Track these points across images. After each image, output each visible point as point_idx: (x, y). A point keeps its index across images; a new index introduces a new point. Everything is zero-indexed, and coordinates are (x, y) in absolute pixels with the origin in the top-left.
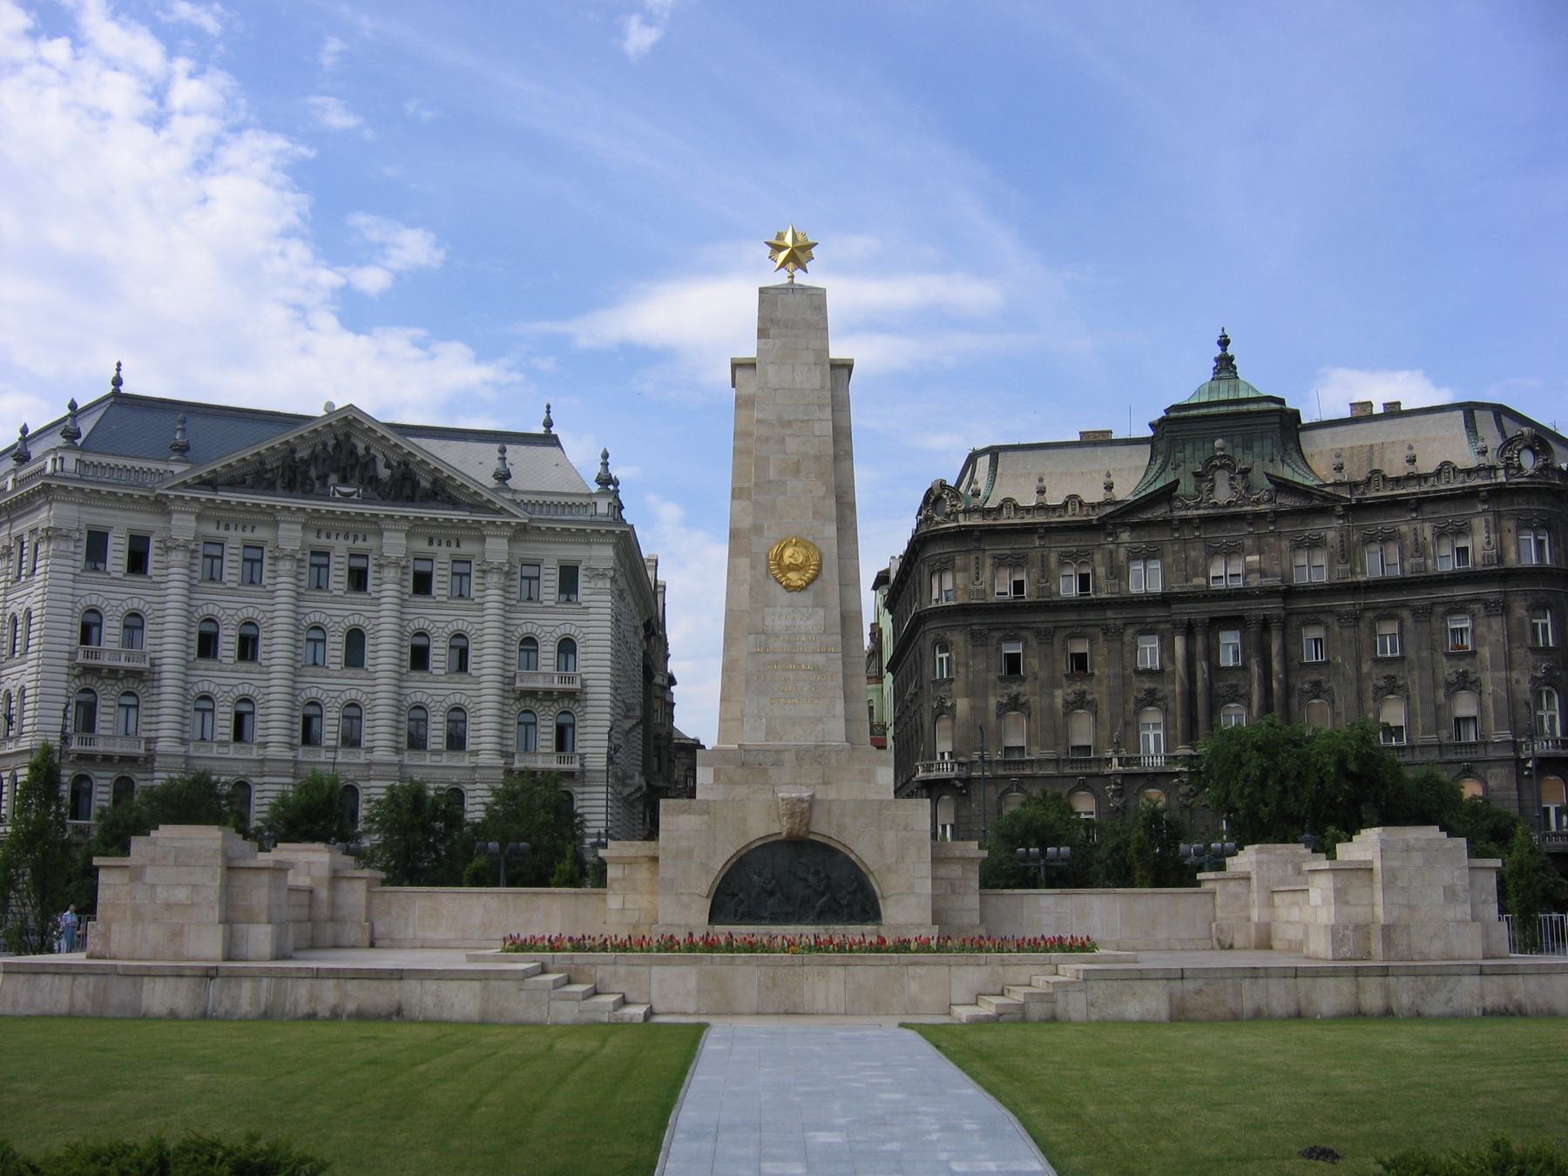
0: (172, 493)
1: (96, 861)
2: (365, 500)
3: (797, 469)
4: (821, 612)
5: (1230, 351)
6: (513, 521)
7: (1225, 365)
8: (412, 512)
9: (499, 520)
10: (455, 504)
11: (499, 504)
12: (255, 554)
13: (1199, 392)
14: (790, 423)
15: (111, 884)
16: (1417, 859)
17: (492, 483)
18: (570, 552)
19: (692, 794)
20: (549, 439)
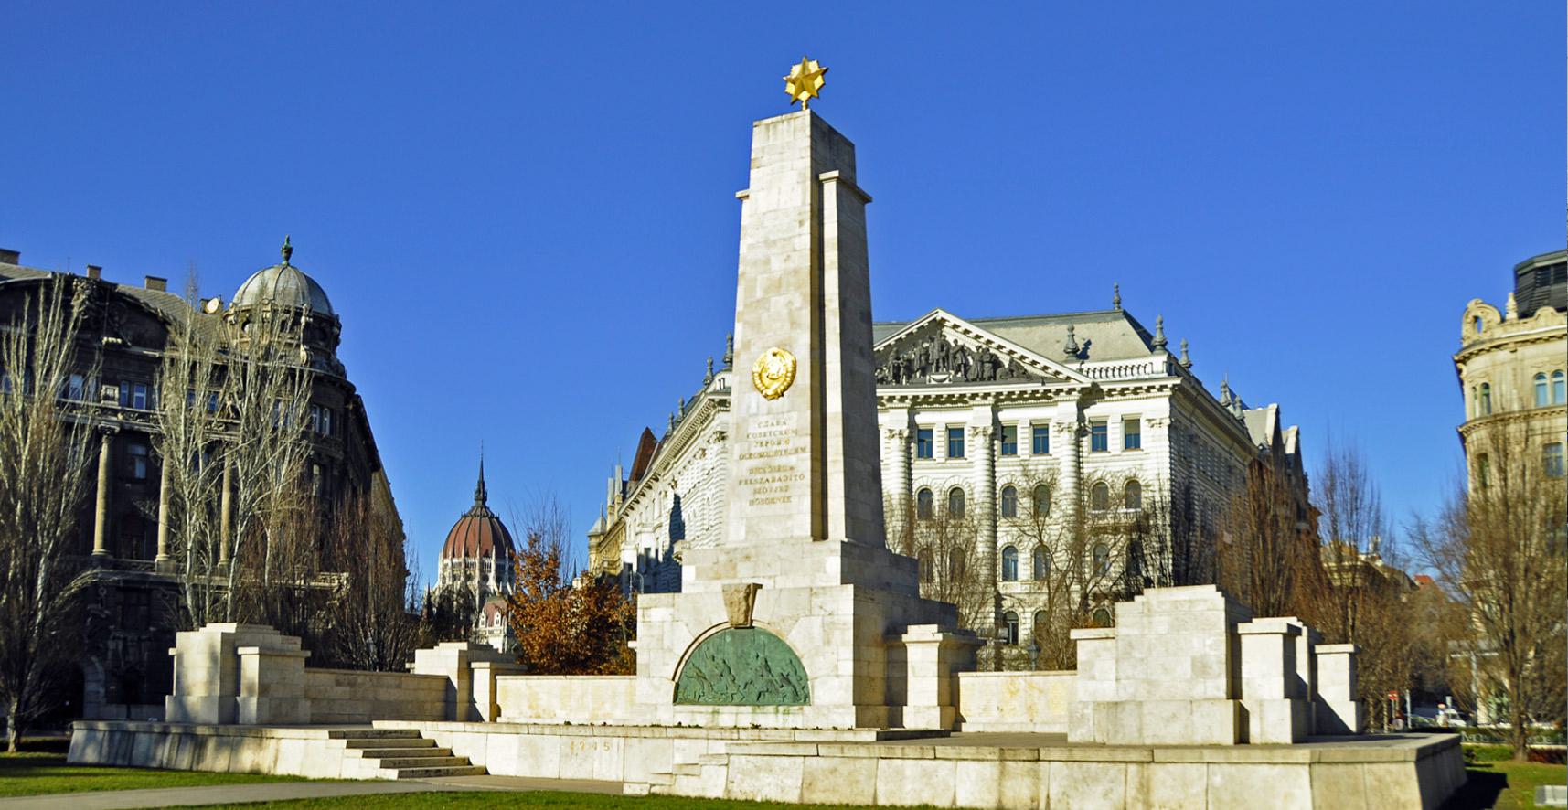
2: (955, 383)
3: (777, 286)
8: (993, 389)
10: (1029, 378)
11: (1065, 373)
19: (678, 590)
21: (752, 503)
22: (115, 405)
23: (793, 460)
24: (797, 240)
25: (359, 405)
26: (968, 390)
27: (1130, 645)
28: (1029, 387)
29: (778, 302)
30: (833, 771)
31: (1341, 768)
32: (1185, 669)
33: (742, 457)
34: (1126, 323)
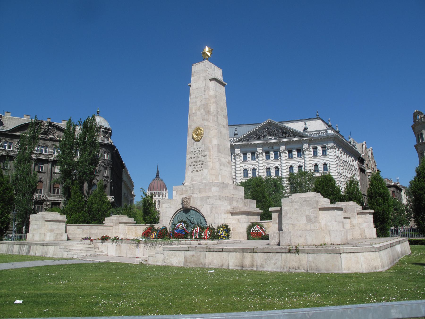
2: (275, 139)
3: (199, 109)
4: (203, 145)
6: (308, 138)
8: (285, 140)
9: (305, 139)
14: (198, 97)
21: (192, 172)
22: (52, 154)
23: (203, 158)
24: (204, 96)
25: (117, 152)
26: (278, 141)
27: (286, 212)
28: (295, 139)
29: (199, 113)
30: (193, 256)
31: (352, 254)
32: (303, 220)
33: (189, 159)
34: (320, 121)
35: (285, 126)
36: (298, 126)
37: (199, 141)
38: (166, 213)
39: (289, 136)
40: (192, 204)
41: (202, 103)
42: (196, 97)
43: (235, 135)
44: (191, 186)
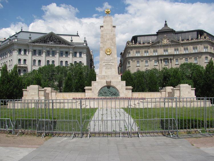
0: (29, 44)
1: (23, 90)
2: (54, 44)
3: (108, 40)
5: (167, 23)
6: (73, 47)
7: (166, 25)
8: (60, 45)
9: (71, 46)
12: (53, 52)
13: (163, 28)
15: (25, 93)
16: (185, 88)
17: (70, 42)
18: (81, 50)
19: (96, 80)
20: (78, 35)
23: (112, 63)
28: (66, 46)
29: (108, 42)
32: (187, 93)
35: (61, 37)
36: (68, 39)
37: (109, 55)
38: (96, 88)
39: (63, 43)
40: (112, 84)
41: (110, 37)
42: (107, 34)
43: (30, 38)
44: (107, 76)
